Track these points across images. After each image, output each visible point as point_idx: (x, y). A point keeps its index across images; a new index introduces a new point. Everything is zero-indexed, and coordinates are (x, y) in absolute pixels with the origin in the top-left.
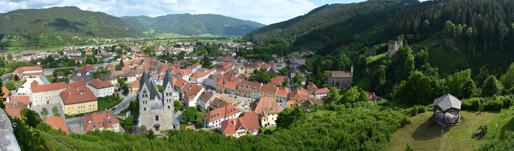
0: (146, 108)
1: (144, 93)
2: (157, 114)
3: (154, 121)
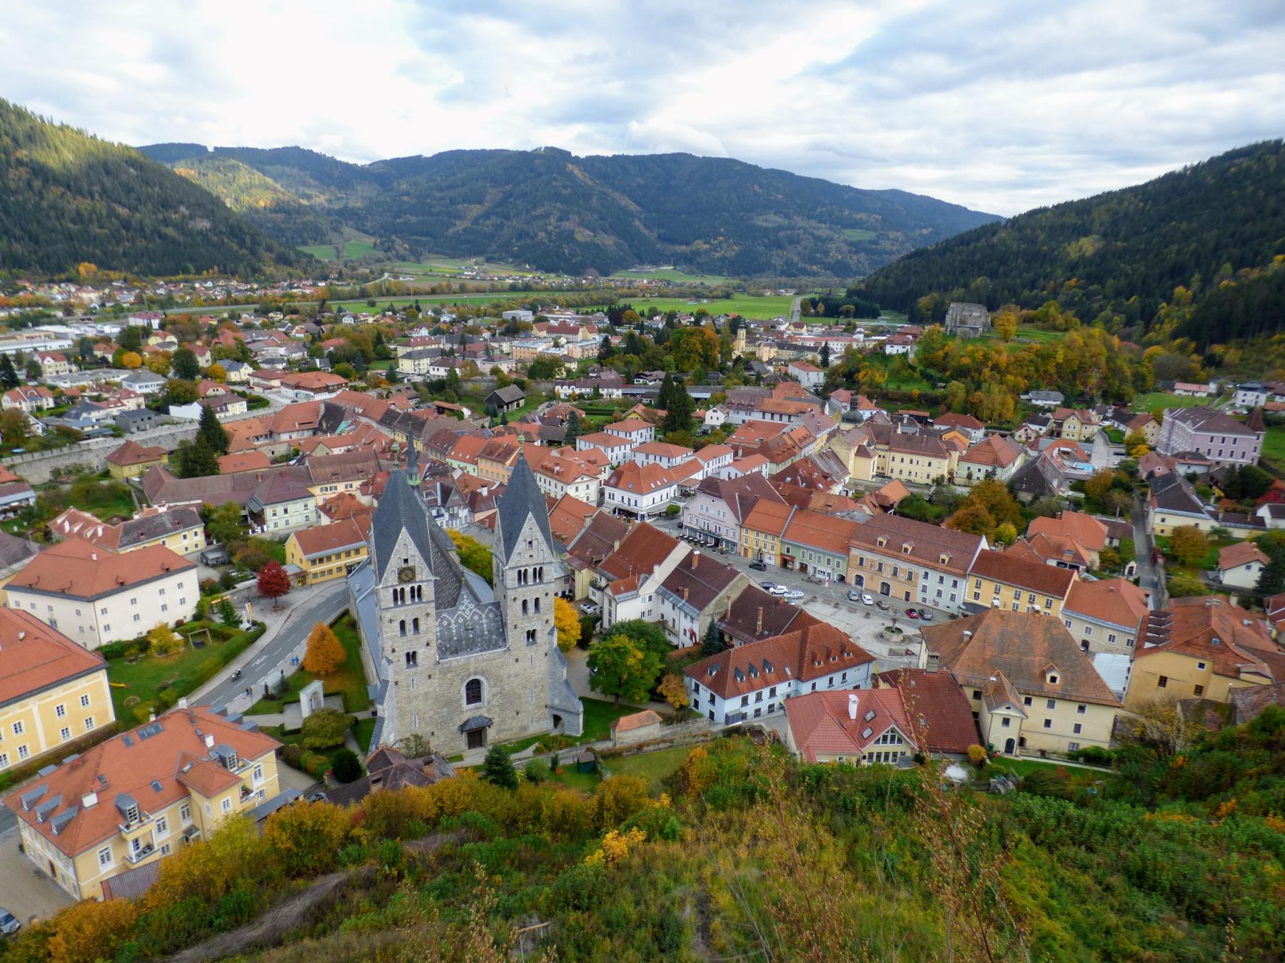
0: (414, 653)
1: (401, 580)
2: (476, 673)
3: (460, 706)
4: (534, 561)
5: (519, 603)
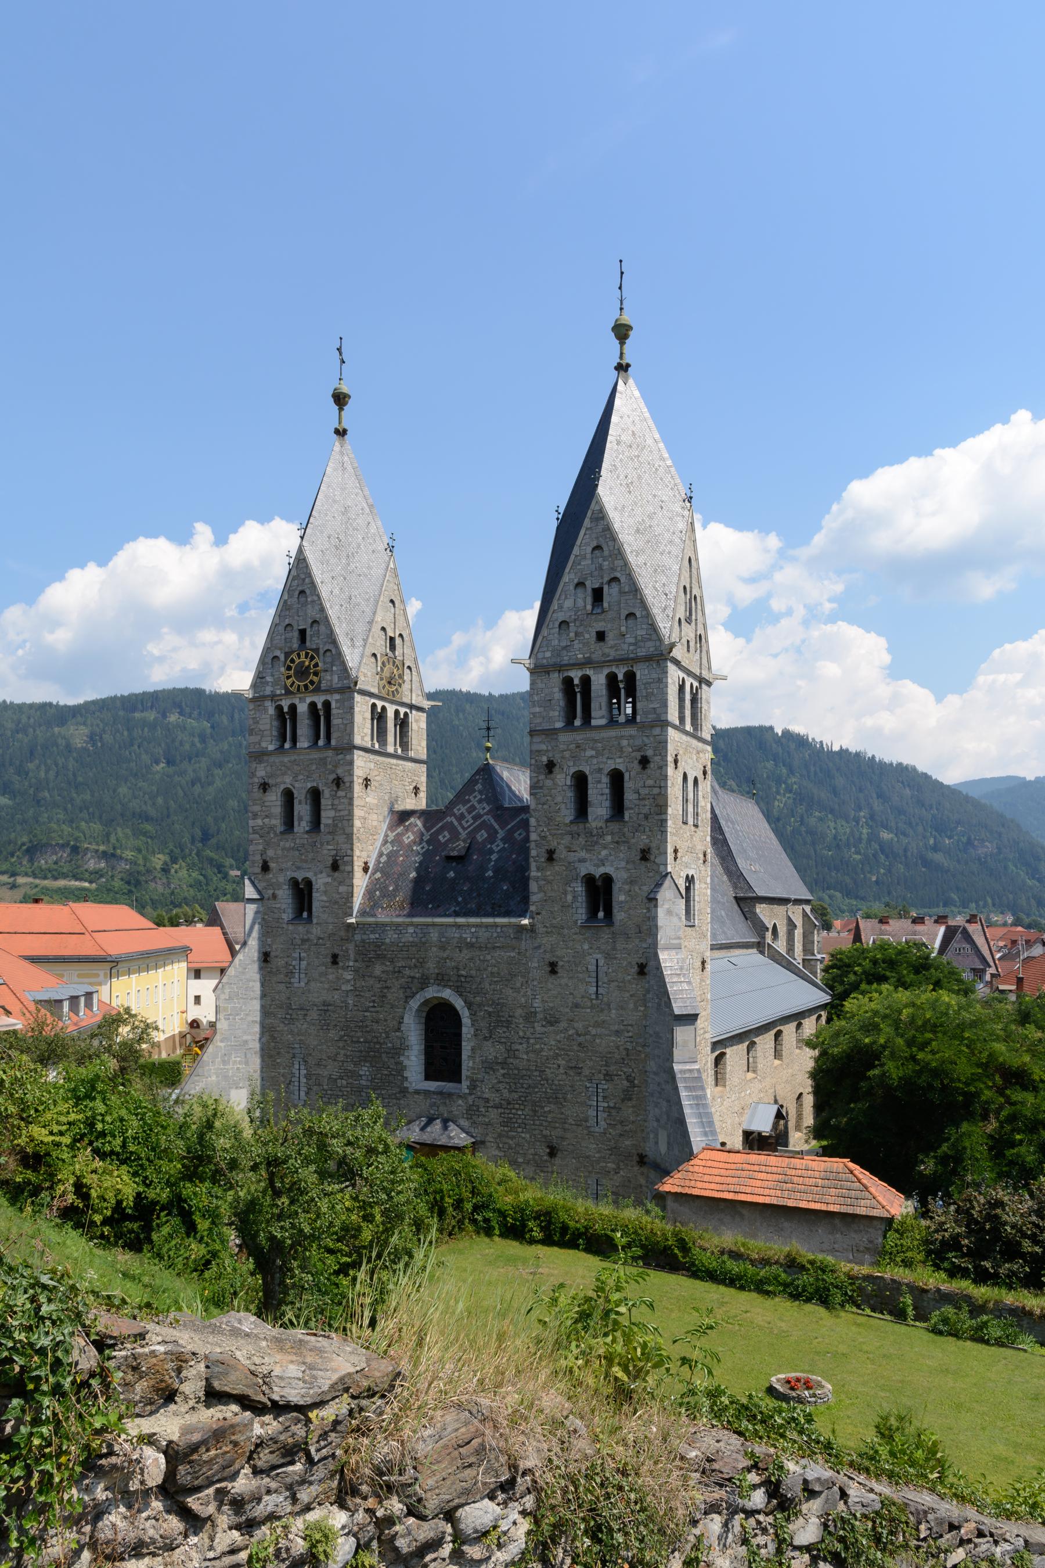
2: (442, 980)
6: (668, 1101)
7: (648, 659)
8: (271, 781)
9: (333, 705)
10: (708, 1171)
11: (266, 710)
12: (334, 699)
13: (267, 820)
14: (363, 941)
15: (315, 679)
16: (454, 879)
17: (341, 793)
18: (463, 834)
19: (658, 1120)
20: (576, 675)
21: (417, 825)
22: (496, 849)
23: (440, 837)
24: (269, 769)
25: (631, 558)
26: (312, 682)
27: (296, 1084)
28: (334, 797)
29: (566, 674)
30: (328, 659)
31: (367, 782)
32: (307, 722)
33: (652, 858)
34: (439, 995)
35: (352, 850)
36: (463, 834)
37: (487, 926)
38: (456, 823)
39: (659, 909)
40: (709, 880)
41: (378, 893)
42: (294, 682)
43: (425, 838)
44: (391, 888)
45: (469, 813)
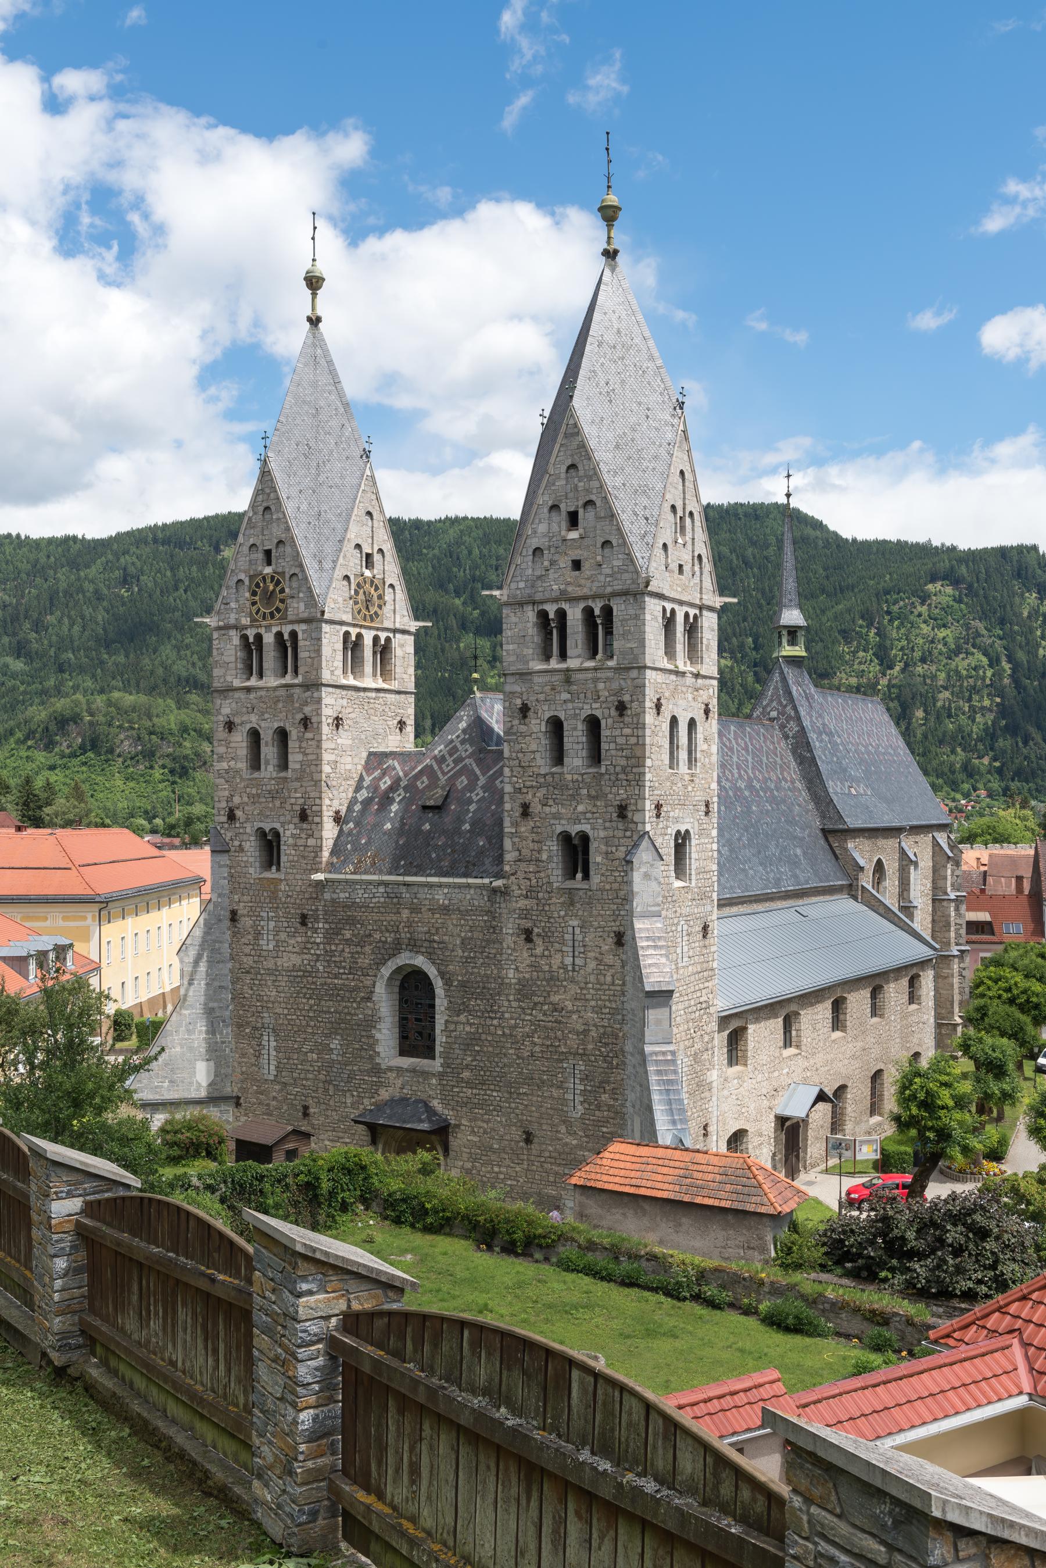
2: (414, 946)
4: (586, 583)
5: (538, 725)
6: (641, 1086)
7: (625, 593)
8: (237, 720)
9: (300, 636)
10: (615, 1164)
11: (230, 639)
12: (300, 628)
13: (232, 763)
14: (333, 901)
15: (281, 606)
16: (429, 832)
17: (309, 735)
18: (443, 779)
19: (634, 1106)
20: (551, 609)
21: (395, 769)
22: (475, 798)
23: (419, 783)
24: (234, 705)
25: (607, 478)
26: (278, 610)
27: (266, 1057)
28: (300, 740)
29: (541, 607)
30: (295, 584)
31: (338, 722)
32: (272, 654)
33: (630, 815)
34: (412, 962)
35: (320, 798)
36: (443, 779)
37: (460, 886)
38: (436, 767)
39: (635, 873)
40: (714, 833)
41: (349, 846)
42: (259, 610)
43: (402, 784)
44: (363, 841)
45: (451, 755)
